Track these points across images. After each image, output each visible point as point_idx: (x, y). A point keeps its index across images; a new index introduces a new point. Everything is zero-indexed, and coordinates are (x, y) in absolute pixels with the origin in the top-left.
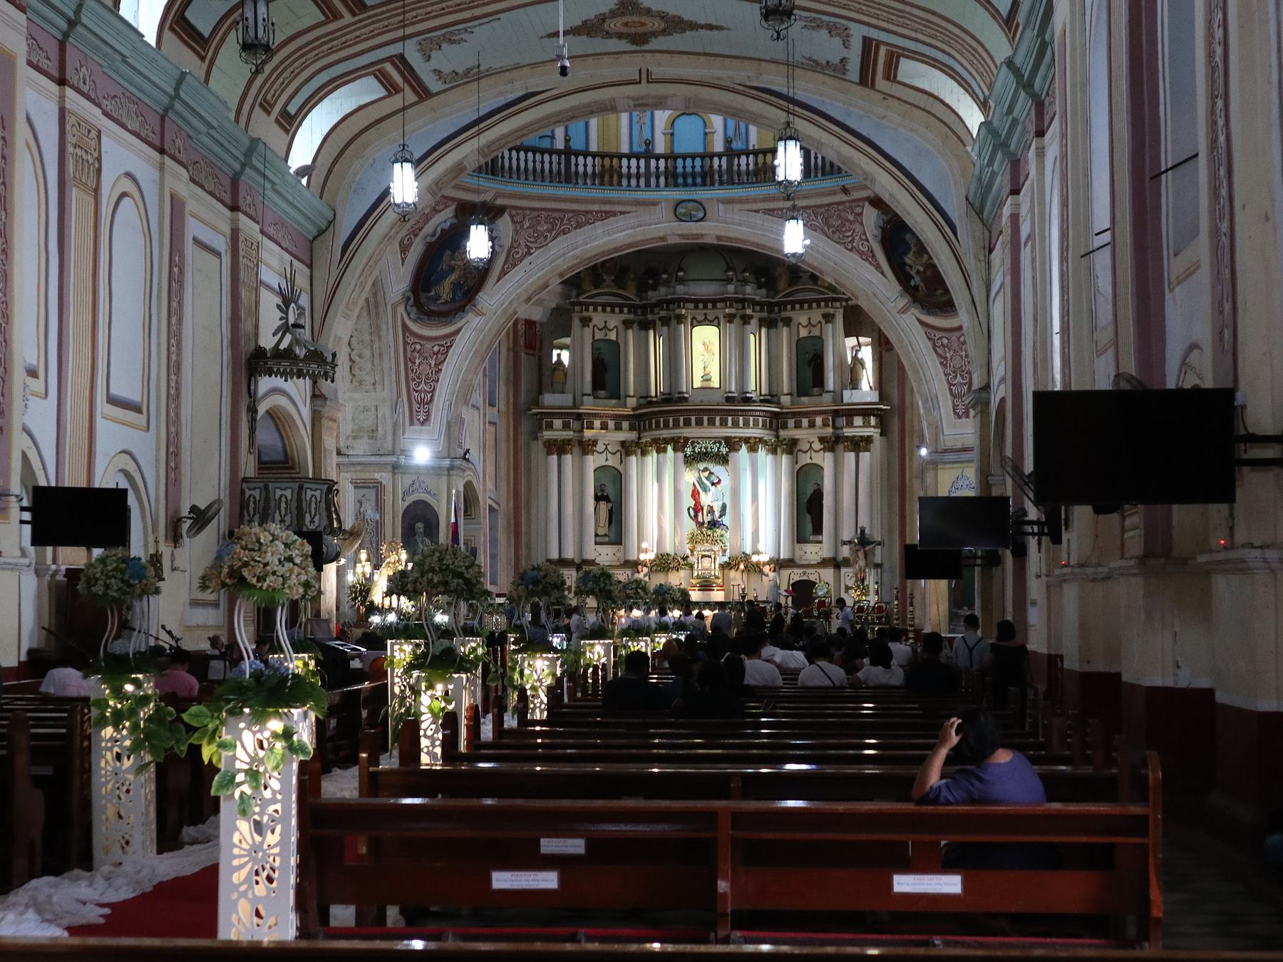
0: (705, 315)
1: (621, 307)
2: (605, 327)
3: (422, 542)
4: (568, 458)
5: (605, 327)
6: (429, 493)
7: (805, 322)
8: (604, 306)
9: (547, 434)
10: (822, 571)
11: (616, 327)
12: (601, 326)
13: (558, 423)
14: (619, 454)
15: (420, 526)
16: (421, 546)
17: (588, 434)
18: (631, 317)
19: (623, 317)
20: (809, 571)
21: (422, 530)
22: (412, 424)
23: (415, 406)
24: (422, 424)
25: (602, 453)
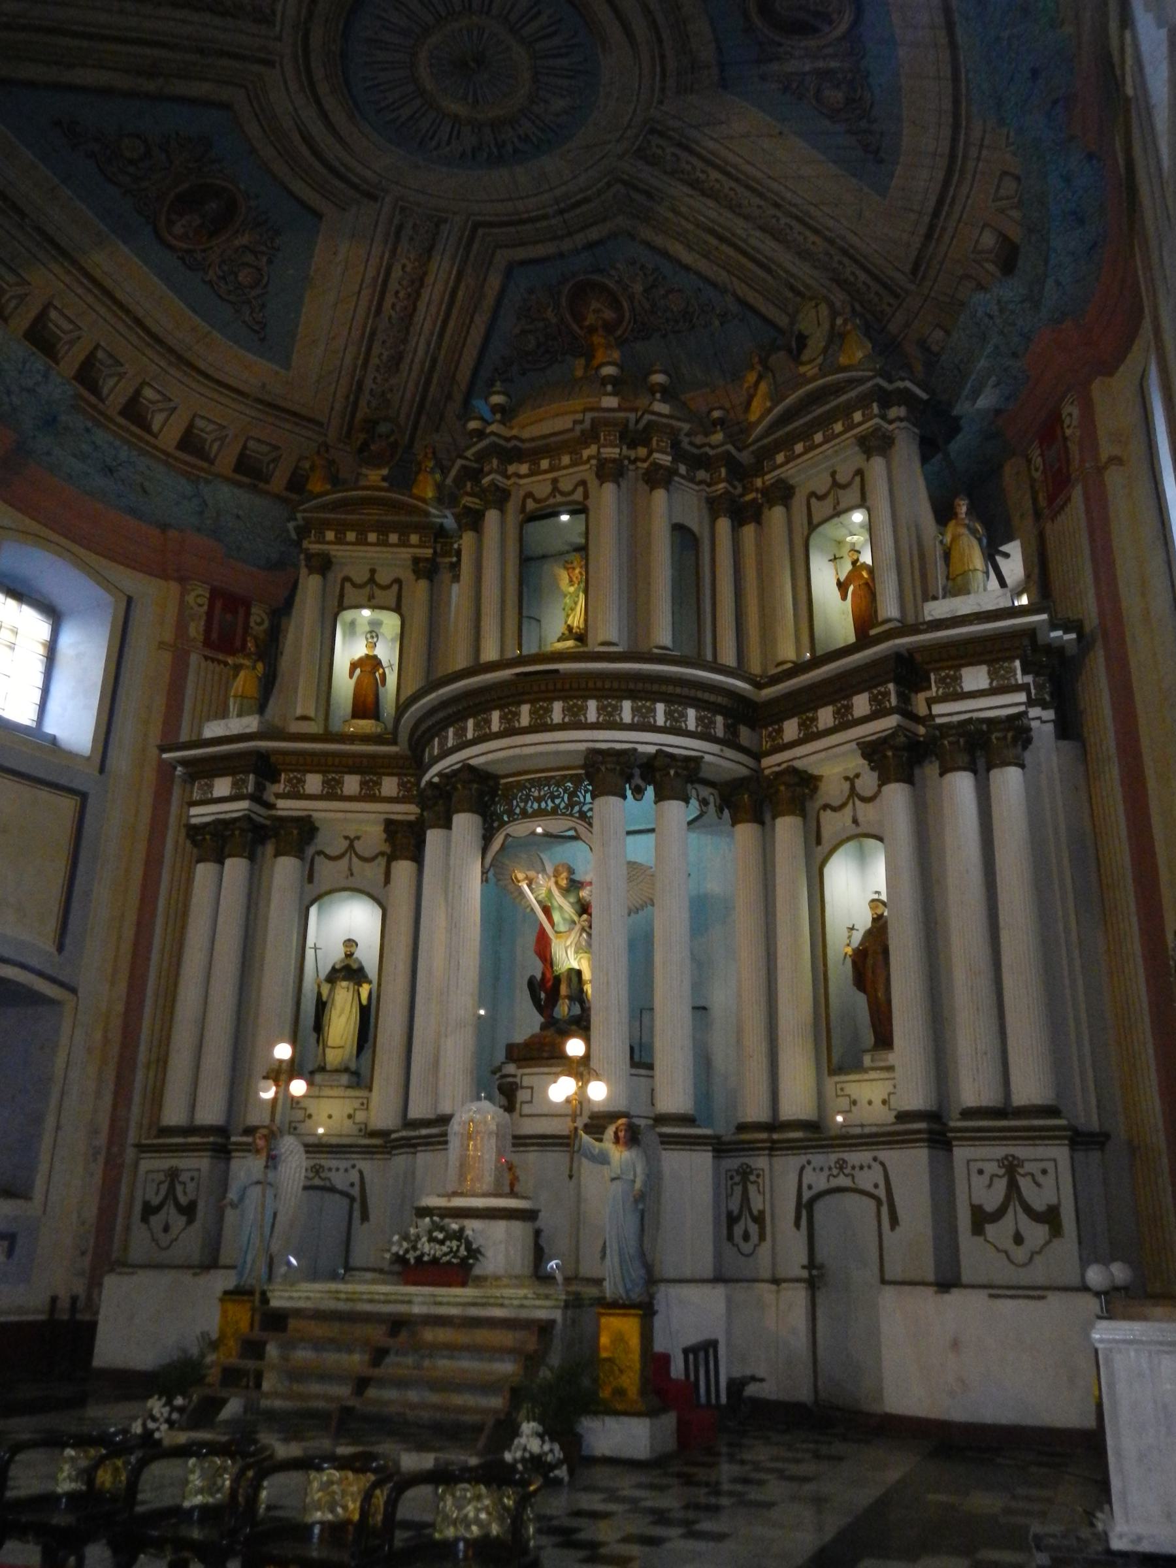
0: (555, 481)
1: (404, 530)
2: (372, 580)
4: (235, 867)
5: (372, 580)
7: (821, 483)
8: (362, 532)
9: (201, 814)
10: (889, 1156)
11: (398, 581)
12: (361, 576)
13: (222, 786)
14: (382, 861)
17: (287, 807)
18: (428, 552)
19: (406, 554)
20: (855, 1157)
25: (341, 856)
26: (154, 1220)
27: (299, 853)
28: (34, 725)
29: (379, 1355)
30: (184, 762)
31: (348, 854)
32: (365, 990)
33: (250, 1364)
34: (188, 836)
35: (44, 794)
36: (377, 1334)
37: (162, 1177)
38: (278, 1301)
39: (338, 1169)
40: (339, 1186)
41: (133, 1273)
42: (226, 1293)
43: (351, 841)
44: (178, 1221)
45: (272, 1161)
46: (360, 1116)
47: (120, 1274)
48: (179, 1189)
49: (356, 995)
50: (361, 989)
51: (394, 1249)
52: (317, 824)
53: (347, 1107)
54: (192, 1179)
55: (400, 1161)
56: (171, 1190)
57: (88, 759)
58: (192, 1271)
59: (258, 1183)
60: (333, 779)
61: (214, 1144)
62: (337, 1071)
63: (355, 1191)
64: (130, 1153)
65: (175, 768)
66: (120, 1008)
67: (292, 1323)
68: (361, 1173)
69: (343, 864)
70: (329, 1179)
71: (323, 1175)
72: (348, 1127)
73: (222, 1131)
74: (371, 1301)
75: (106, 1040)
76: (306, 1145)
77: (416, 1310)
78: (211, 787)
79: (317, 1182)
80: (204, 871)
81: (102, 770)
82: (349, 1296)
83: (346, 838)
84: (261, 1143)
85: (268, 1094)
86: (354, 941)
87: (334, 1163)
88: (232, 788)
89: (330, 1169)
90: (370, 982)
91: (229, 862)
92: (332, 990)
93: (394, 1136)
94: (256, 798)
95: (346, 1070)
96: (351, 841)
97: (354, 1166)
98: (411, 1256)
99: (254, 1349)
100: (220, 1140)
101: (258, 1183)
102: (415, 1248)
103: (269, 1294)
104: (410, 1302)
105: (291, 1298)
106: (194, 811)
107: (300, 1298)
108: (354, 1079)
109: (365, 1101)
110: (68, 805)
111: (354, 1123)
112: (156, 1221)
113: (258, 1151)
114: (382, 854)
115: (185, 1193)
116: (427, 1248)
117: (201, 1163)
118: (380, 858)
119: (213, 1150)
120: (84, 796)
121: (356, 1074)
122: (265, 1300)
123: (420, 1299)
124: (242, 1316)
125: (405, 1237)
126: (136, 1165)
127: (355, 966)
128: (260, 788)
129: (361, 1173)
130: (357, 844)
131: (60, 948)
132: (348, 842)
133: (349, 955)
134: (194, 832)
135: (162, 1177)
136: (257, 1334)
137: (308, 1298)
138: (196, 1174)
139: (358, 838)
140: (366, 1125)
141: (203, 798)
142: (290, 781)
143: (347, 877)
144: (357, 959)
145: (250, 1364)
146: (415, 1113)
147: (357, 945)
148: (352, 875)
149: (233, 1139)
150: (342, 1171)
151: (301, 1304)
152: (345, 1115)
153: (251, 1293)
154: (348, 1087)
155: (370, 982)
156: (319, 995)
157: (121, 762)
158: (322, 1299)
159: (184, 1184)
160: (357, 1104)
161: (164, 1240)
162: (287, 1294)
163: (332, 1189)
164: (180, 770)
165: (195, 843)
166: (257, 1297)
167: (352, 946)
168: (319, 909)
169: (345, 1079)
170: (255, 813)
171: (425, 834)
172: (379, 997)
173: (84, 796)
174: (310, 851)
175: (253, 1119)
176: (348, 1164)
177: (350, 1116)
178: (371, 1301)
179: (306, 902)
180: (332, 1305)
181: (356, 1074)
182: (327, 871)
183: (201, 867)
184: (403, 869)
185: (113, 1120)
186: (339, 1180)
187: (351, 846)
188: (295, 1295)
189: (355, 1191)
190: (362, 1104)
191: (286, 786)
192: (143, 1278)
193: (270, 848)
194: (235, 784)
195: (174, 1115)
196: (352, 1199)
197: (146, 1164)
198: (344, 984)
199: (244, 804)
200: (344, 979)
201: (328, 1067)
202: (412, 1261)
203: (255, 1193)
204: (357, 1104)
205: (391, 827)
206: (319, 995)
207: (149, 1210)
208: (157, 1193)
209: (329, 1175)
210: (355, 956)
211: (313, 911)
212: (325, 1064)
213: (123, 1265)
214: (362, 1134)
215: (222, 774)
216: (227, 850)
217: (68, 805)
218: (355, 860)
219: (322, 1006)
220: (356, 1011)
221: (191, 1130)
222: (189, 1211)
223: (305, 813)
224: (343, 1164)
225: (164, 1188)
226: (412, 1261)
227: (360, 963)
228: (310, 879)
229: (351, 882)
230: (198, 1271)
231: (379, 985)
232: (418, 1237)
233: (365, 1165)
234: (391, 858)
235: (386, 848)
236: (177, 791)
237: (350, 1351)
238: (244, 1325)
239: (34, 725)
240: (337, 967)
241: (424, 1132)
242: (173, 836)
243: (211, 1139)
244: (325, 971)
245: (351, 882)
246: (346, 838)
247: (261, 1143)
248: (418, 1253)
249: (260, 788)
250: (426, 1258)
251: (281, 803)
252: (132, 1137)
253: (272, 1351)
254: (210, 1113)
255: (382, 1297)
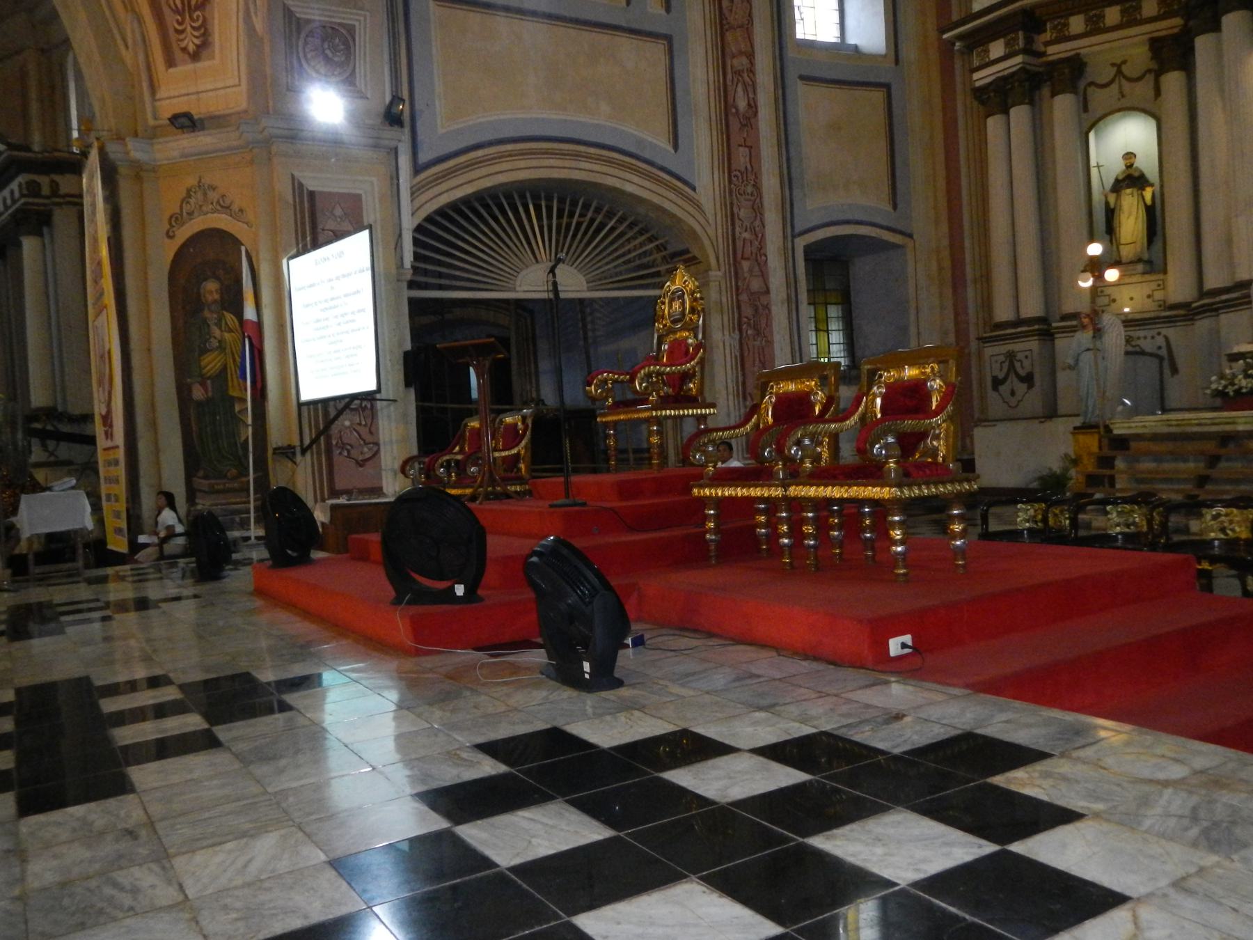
3: (219, 325)
4: (1020, 115)
6: (227, 208)
9: (982, 77)
13: (997, 49)
14: (1150, 78)
15: (211, 288)
16: (217, 332)
17: (1057, 51)
21: (217, 296)
22: (170, 62)
23: (171, 19)
24: (195, 57)
26: (1002, 388)
27: (1073, 89)
28: (839, 41)
29: (1214, 460)
30: (960, 37)
31: (1117, 78)
32: (1148, 193)
33: (1107, 472)
34: (976, 98)
35: (860, 93)
36: (1210, 447)
37: (1002, 358)
38: (1119, 429)
39: (1145, 338)
40: (1148, 350)
41: (994, 425)
42: (1075, 428)
43: (1118, 67)
44: (1021, 388)
45: (1098, 332)
46: (1159, 295)
47: (985, 426)
48: (1017, 365)
49: (1141, 199)
50: (1144, 193)
51: (1214, 386)
52: (1085, 60)
53: (1146, 289)
54: (1026, 357)
55: (1203, 325)
56: (1012, 366)
57: (885, 56)
58: (1037, 421)
59: (1088, 350)
60: (1095, 15)
61: (1037, 330)
62: (1131, 262)
63: (1164, 352)
64: (974, 345)
65: (954, 44)
66: (945, 242)
67: (1133, 444)
68: (1166, 338)
69: (1115, 87)
70: (1138, 345)
71: (1133, 343)
72: (1150, 305)
73: (1043, 320)
74: (1199, 425)
75: (940, 269)
76: (1124, 322)
77: (1240, 428)
78: (987, 51)
79: (1130, 349)
80: (994, 124)
81: (897, 61)
82: (1179, 422)
83: (1113, 65)
84: (1086, 321)
85: (1086, 283)
86: (1132, 153)
87: (1141, 334)
88: (1006, 48)
89: (1139, 338)
90: (1152, 185)
91: (1013, 111)
92: (1118, 198)
93: (1194, 305)
94: (1027, 51)
95: (1140, 260)
96: (1118, 67)
97: (1159, 334)
98: (1230, 390)
99: (1106, 461)
100: (1045, 327)
101: (1088, 350)
102: (1233, 384)
103: (1111, 426)
104: (1234, 423)
105: (1130, 427)
106: (976, 76)
107: (1136, 427)
108: (1148, 268)
109: (1161, 282)
110: (878, 96)
111: (1154, 301)
112: (1004, 388)
113: (1084, 327)
114: (1149, 71)
115: (1022, 367)
116: (1244, 383)
117: (1033, 344)
118: (1148, 76)
119: (1039, 335)
120: (887, 87)
121: (1149, 262)
122: (1108, 429)
123: (1243, 420)
124: (1091, 442)
125: (1222, 377)
126: (980, 354)
127: (1136, 174)
128: (1029, 41)
129: (1166, 338)
130: (1124, 68)
131: (895, 207)
132: (1115, 68)
133: (1130, 166)
134: (980, 93)
135: (1002, 358)
136: (1107, 452)
137: (1145, 426)
138: (1027, 353)
139: (1124, 62)
140: (1164, 302)
141: (983, 62)
142: (1054, 28)
143: (1119, 99)
144: (1137, 169)
145: (1107, 472)
146: (1211, 283)
147: (1135, 156)
148: (1123, 96)
149: (1054, 325)
150: (1149, 338)
151: (1140, 431)
152: (1145, 296)
153: (1096, 426)
154: (1144, 273)
155: (1152, 185)
156: (1107, 203)
157: (910, 52)
158: (1156, 426)
159: (1020, 361)
160: (1154, 286)
161: (1013, 401)
162: (1126, 425)
163: (1143, 353)
164: (958, 45)
165: (982, 103)
166: (1102, 430)
167: (1130, 158)
168: (1096, 134)
169: (1140, 267)
170: (1030, 64)
171: (1193, 42)
172: (1162, 195)
173: (887, 87)
174: (1082, 84)
175: (1068, 308)
176: (1154, 332)
177: (1149, 296)
178: (1199, 425)
179: (1085, 130)
180: (1165, 430)
181: (1149, 262)
182: (1099, 98)
183: (990, 121)
184: (1173, 81)
185: (957, 323)
186: (1147, 345)
187: (1119, 72)
188: (1133, 425)
189: (1164, 352)
190: (1159, 285)
191: (1052, 33)
192: (1001, 427)
193: (1046, 91)
194: (1007, 45)
195: (1003, 312)
196: (1161, 359)
197: (989, 350)
198: (1129, 191)
199: (1019, 59)
200: (1128, 187)
201: (1124, 260)
202: (1231, 394)
203: (1087, 358)
204: (1154, 286)
205: (1156, 45)
206: (1107, 203)
207: (997, 383)
208: (1001, 370)
209: (1139, 342)
210: (1134, 166)
211: (1092, 136)
212: (1120, 257)
213: (985, 421)
214: (1162, 308)
215: (994, 38)
216: (1010, 101)
217: (878, 96)
218: (1124, 82)
219: (1111, 213)
220: (1142, 213)
221: (1019, 322)
222: (1028, 379)
223: (1072, 53)
224: (1149, 333)
225: (1006, 366)
226: (1231, 394)
227: (1141, 171)
228: (1086, 109)
229: (1124, 103)
230: (1043, 420)
231: (1162, 186)
232: (1234, 376)
233: (1171, 332)
234: (1158, 73)
235: (1154, 65)
236: (958, 64)
237: (1185, 461)
238: (1095, 449)
239: (839, 41)
240: (1120, 178)
241: (1224, 297)
242: (962, 101)
243: (1036, 327)
244: (1109, 182)
245: (1124, 103)
246: (1113, 65)
247: (1086, 321)
248: (1236, 387)
249: (1029, 41)
250: (1244, 390)
251: (1051, 49)
252: (972, 336)
253: (1120, 464)
254: (1032, 307)
255: (1209, 422)
